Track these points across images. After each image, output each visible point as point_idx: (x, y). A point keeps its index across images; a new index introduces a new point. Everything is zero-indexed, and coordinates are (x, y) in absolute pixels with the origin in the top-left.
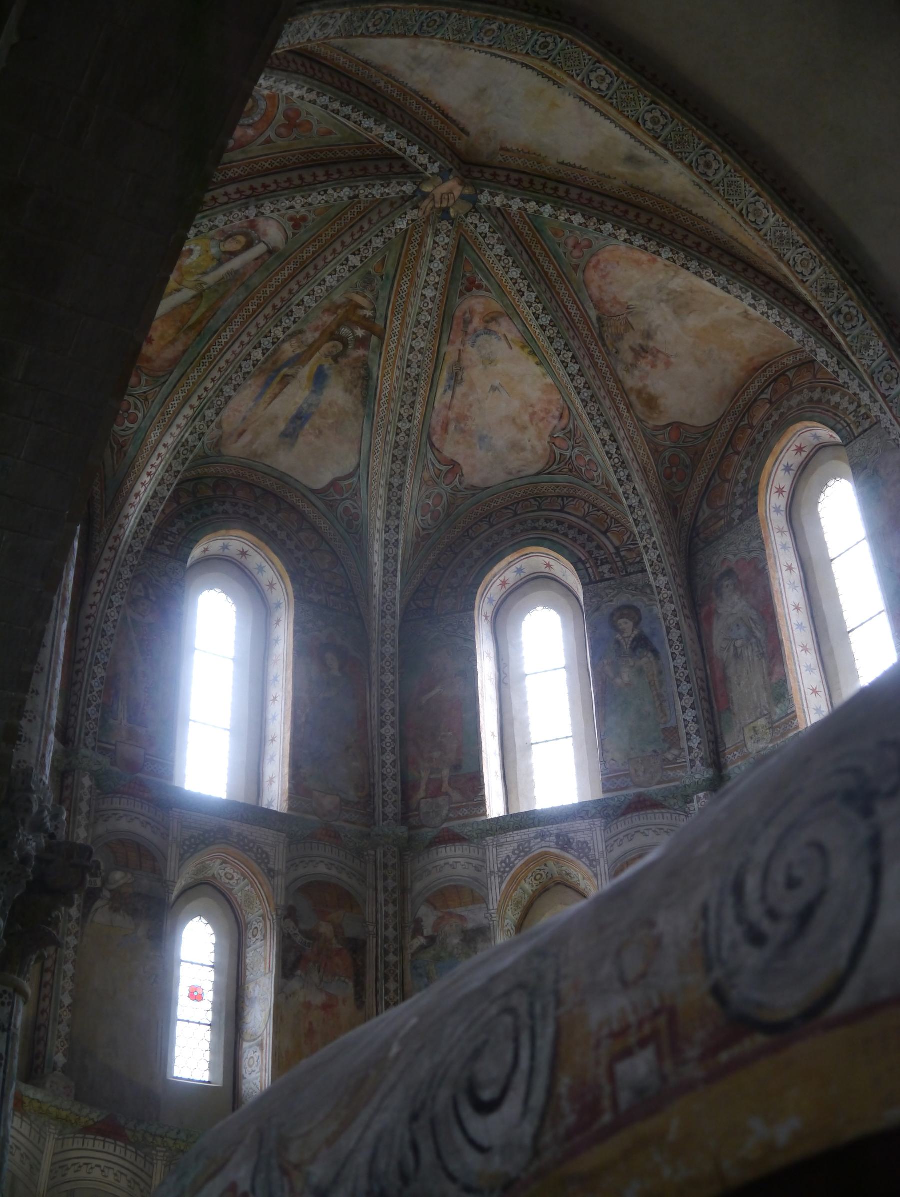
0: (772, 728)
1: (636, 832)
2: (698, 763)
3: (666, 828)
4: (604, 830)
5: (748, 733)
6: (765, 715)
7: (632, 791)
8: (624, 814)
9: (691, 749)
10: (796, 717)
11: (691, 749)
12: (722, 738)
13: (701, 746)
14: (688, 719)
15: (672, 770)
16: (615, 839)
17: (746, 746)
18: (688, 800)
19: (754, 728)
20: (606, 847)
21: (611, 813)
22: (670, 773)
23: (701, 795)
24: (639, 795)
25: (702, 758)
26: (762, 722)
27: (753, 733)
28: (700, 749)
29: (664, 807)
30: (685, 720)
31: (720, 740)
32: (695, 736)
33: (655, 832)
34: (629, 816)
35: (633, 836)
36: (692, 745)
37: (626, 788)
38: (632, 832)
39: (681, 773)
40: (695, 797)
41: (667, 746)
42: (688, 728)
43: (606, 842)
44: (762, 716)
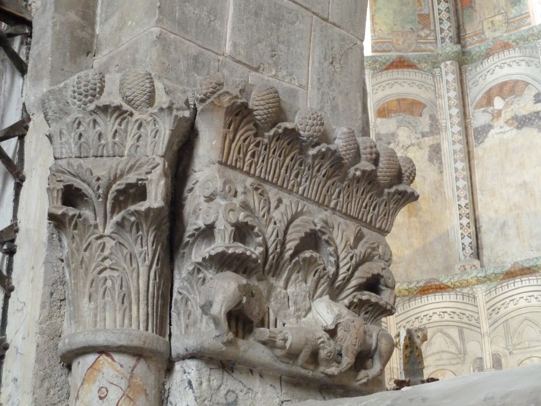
0: (508, 22)
1: (395, 83)
2: (447, 40)
3: (417, 83)
4: (372, 78)
5: (486, 25)
6: (502, 13)
7: (394, 55)
8: (387, 69)
9: (442, 30)
10: (529, 16)
11: (442, 30)
12: (463, 26)
13: (450, 29)
14: (441, 8)
15: (424, 43)
16: (379, 85)
17: (483, 33)
18: (435, 65)
19: (492, 22)
20: (373, 90)
21: (378, 66)
22: (422, 45)
23: (448, 62)
24: (401, 57)
25: (451, 37)
26: (499, 18)
27: (490, 25)
28: (450, 31)
29: (416, 68)
30: (439, 9)
31: (461, 27)
32: (446, 21)
33: (409, 84)
34: (390, 71)
35: (393, 85)
36: (443, 27)
37: (389, 51)
38: (392, 82)
39: (430, 47)
40: (442, 65)
41: (421, 26)
42: (441, 15)
43: (373, 86)
44: (499, 13)
